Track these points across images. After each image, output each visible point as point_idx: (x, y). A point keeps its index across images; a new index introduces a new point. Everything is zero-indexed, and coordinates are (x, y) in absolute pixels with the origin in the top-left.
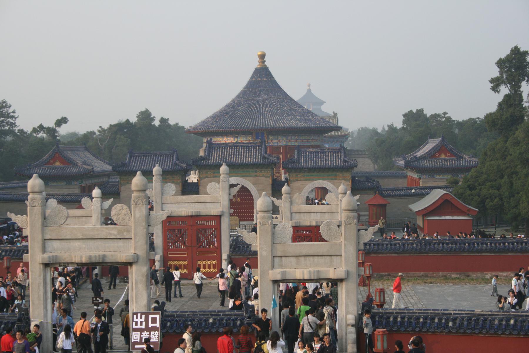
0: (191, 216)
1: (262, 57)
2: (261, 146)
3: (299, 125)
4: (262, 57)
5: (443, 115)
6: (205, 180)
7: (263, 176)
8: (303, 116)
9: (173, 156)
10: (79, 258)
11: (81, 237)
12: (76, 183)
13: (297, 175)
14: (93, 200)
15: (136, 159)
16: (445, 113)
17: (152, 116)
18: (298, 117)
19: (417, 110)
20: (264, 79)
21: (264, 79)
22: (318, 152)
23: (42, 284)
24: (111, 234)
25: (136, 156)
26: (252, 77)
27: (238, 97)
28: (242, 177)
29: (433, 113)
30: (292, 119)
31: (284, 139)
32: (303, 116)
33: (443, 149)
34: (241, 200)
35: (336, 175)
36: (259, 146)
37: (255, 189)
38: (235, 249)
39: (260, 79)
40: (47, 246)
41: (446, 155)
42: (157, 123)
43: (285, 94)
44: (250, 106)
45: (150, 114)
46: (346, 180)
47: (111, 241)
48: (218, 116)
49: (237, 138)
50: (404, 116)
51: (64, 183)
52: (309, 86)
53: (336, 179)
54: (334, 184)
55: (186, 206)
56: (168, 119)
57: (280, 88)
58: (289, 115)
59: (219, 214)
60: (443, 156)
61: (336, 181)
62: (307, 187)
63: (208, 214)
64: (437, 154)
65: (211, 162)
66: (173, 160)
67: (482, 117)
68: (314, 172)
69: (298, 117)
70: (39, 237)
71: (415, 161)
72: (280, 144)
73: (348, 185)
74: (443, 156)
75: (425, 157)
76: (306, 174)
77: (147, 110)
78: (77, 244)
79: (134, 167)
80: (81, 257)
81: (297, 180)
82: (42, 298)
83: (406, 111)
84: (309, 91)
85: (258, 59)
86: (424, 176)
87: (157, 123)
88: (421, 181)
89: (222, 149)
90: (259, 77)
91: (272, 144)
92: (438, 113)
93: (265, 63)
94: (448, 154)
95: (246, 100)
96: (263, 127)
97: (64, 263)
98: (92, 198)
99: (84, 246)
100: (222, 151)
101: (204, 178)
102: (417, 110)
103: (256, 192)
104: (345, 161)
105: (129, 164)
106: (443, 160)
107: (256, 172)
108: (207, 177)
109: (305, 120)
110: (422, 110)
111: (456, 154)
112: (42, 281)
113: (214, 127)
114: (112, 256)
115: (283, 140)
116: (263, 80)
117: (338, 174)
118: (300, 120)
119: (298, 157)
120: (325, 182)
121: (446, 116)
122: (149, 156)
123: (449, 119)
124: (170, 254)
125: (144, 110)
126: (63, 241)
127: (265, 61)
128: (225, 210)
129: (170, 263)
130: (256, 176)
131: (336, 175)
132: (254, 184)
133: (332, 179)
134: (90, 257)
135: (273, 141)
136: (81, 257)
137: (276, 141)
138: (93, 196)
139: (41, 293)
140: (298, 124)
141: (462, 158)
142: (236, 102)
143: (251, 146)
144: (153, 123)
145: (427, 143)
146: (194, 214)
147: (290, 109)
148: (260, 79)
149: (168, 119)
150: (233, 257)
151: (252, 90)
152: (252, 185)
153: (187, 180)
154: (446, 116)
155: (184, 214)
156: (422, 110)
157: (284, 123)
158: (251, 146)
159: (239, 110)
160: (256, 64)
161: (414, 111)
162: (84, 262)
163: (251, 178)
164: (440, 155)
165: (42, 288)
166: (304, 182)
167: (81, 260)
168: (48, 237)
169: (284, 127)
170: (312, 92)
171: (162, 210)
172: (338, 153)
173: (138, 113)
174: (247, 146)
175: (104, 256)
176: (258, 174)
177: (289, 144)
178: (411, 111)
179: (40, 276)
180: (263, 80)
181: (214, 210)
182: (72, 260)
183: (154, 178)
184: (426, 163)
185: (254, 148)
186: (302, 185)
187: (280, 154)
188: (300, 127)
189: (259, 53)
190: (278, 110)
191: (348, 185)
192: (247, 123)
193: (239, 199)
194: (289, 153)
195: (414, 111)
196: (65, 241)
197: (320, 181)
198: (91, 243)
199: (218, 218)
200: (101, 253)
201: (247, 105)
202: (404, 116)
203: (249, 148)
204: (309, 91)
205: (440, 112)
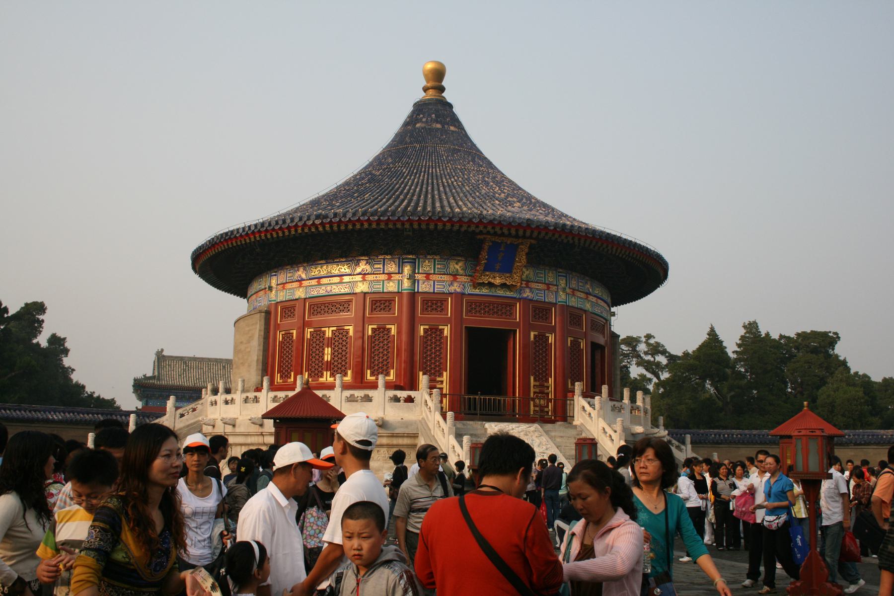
1: (437, 76)
4: (437, 76)
31: (562, 283)
39: (439, 126)
42: (42, 340)
49: (413, 262)
72: (551, 298)
87: (42, 340)
91: (527, 294)
135: (533, 285)
137: (541, 286)
144: (35, 341)
160: (415, 91)
177: (573, 302)
189: (430, 66)
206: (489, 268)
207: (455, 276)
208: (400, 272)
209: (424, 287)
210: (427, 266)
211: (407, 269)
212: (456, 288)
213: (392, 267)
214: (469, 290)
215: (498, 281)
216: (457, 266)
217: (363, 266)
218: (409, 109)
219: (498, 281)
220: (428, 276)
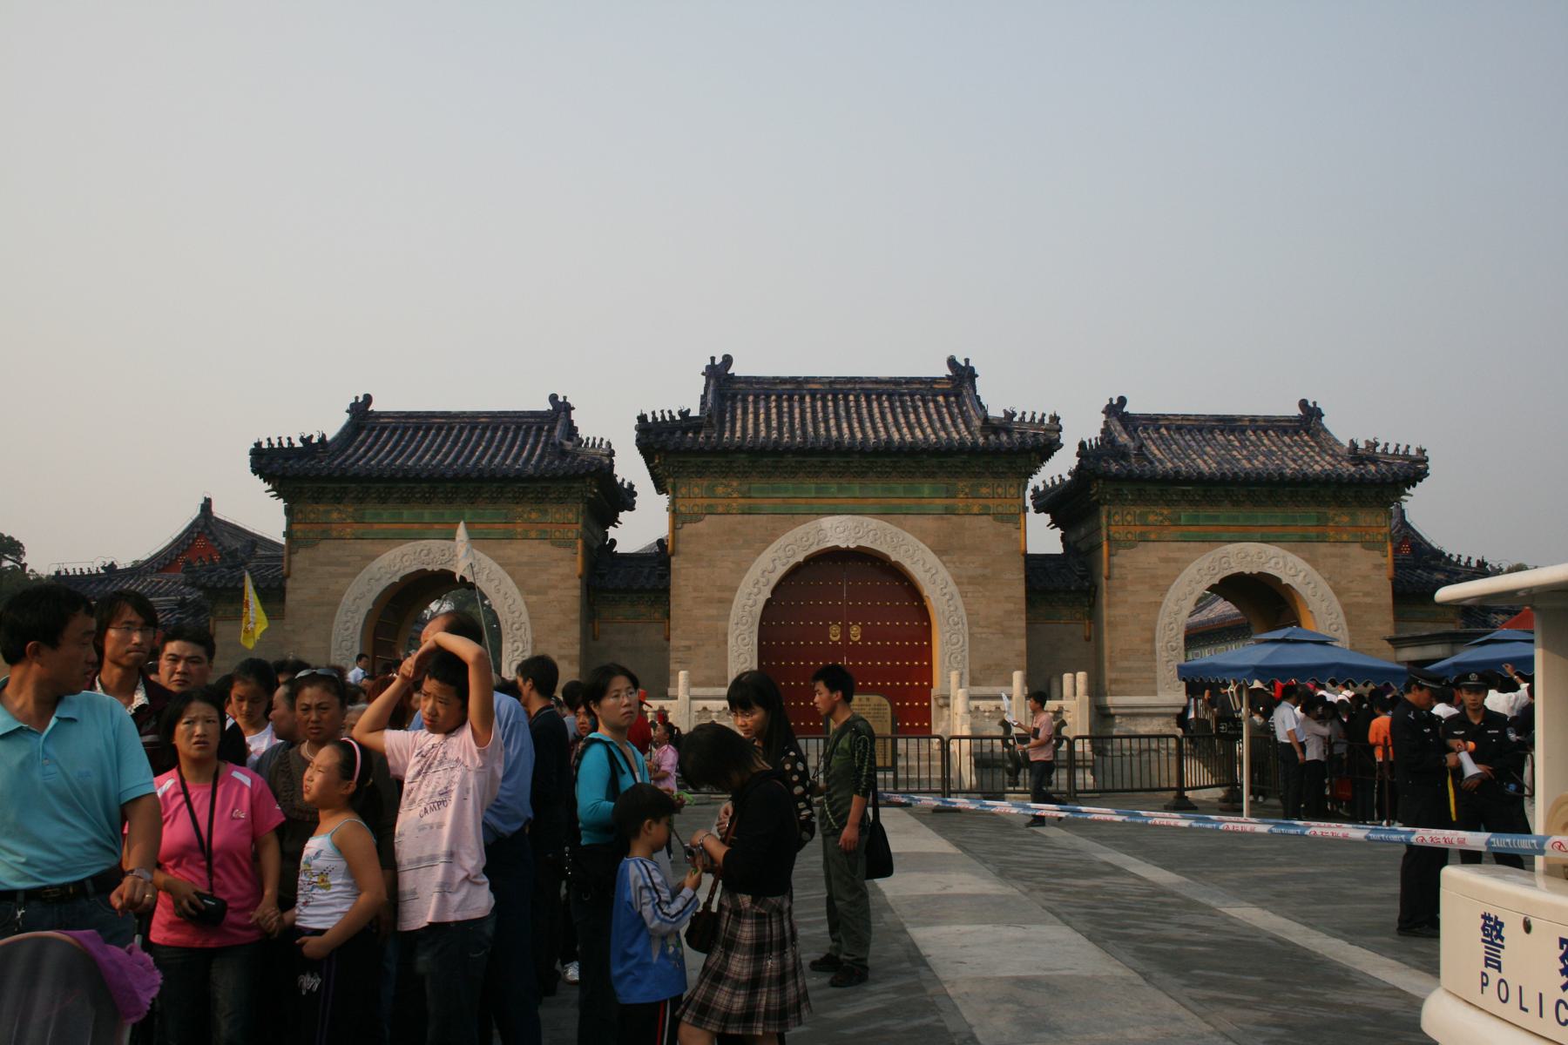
6: (701, 526)
7: (985, 512)
28: (884, 513)
36: (946, 396)
37: (944, 574)
46: (1369, 545)
53: (1321, 539)
54: (1311, 561)
61: (1323, 548)
62: (1191, 571)
73: (1378, 567)
81: (1144, 539)
100: (779, 407)
101: (696, 518)
103: (952, 588)
107: (952, 495)
117: (1331, 513)
120: (1271, 549)
130: (950, 511)
132: (939, 551)
133: (1305, 539)
143: (912, 395)
152: (932, 558)
153: (613, 542)
158: (912, 395)
163: (928, 523)
166: (1173, 549)
176: (960, 503)
186: (1166, 560)
191: (1378, 567)
197: (1252, 548)
203: (903, 403)
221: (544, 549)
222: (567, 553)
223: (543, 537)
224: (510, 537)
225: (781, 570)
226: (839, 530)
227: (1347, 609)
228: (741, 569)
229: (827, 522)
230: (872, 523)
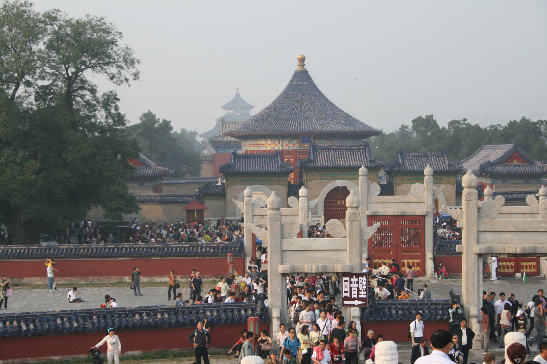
0: (397, 216)
2: (365, 149)
3: (346, 130)
4: (302, 60)
5: (462, 122)
8: (347, 120)
9: (277, 157)
10: (513, 248)
11: (513, 230)
12: (149, 184)
13: (403, 178)
14: (300, 199)
15: (240, 161)
16: (465, 120)
17: (156, 118)
18: (343, 122)
19: (427, 116)
20: (305, 83)
21: (305, 83)
22: (421, 156)
23: (476, 273)
24: (541, 227)
25: (240, 158)
26: (292, 81)
27: (278, 100)
28: (349, 179)
29: (453, 120)
30: (338, 123)
32: (347, 120)
33: (515, 155)
34: (337, 202)
35: (441, 179)
38: (439, 248)
39: (300, 83)
40: (480, 237)
41: (519, 161)
43: (326, 99)
44: (293, 109)
45: (154, 116)
46: (451, 184)
47: (540, 234)
48: (261, 119)
49: (282, 141)
50: (413, 122)
51: (136, 184)
52: (238, 90)
53: (440, 183)
55: (391, 206)
56: (170, 122)
57: (320, 92)
58: (334, 119)
59: (424, 214)
60: (515, 162)
63: (413, 214)
64: (510, 160)
65: (318, 164)
66: (277, 162)
67: (504, 124)
68: (419, 176)
69: (343, 122)
70: (475, 229)
71: (489, 167)
74: (515, 162)
75: (498, 162)
76: (412, 177)
77: (149, 111)
78: (508, 236)
79: (240, 168)
80: (516, 248)
81: (403, 183)
82: (476, 286)
83: (415, 117)
84: (238, 95)
85: (297, 63)
86: (497, 181)
88: (494, 185)
89: (326, 152)
90: (300, 81)
92: (457, 119)
93: (305, 67)
94: (521, 160)
95: (289, 104)
96: (310, 131)
97: (496, 254)
98: (298, 197)
99: (515, 238)
101: (311, 181)
102: (427, 116)
104: (450, 166)
105: (235, 165)
106: (515, 167)
108: (314, 179)
109: (350, 124)
110: (431, 116)
111: (528, 160)
112: (476, 270)
113: (259, 130)
114: (543, 247)
115: (279, 144)
116: (302, 83)
118: (346, 125)
119: (402, 161)
121: (466, 122)
122: (252, 158)
123: (469, 124)
124: (375, 252)
125: (146, 112)
126: (495, 233)
127: (304, 65)
128: (429, 210)
129: (375, 261)
131: (441, 179)
134: (524, 248)
136: (516, 248)
138: (300, 195)
139: (476, 281)
140: (343, 128)
141: (534, 164)
142: (277, 105)
145: (481, 149)
146: (395, 214)
147: (333, 113)
148: (300, 83)
149: (170, 122)
150: (437, 256)
151: (293, 94)
154: (466, 122)
155: (389, 213)
156: (431, 116)
157: (330, 127)
158: (355, 149)
159: (283, 113)
160: (295, 67)
161: (424, 117)
162: (518, 252)
164: (512, 161)
165: (476, 277)
167: (515, 251)
168: (482, 229)
169: (332, 131)
170: (241, 96)
171: (368, 210)
172: (440, 157)
173: (141, 115)
174: (350, 150)
175: (536, 247)
178: (420, 117)
179: (475, 265)
180: (302, 83)
181: (418, 210)
182: (505, 251)
183: (426, 178)
184: (499, 169)
185: (358, 151)
187: (292, 158)
188: (346, 132)
189: (299, 57)
190: (322, 114)
192: (294, 127)
193: (339, 202)
194: (286, 158)
195: (424, 117)
196: (497, 233)
198: (521, 235)
199: (423, 217)
200: (533, 245)
201: (289, 109)
202: (413, 122)
204: (238, 95)
205: (460, 118)
206: (303, 142)
207: (294, 145)
208: (279, 144)
209: (286, 148)
210: (286, 142)
211: (281, 143)
212: (295, 148)
213: (277, 142)
214: (299, 148)
215: (306, 146)
216: (295, 142)
217: (269, 142)
218: (293, 73)
219: (306, 146)
220: (287, 145)
221: (280, 186)
222: (284, 187)
223: (279, 184)
224: (272, 184)
225: (328, 191)
226: (340, 183)
227: (446, 197)
228: (320, 191)
229: (338, 181)
230: (347, 181)
